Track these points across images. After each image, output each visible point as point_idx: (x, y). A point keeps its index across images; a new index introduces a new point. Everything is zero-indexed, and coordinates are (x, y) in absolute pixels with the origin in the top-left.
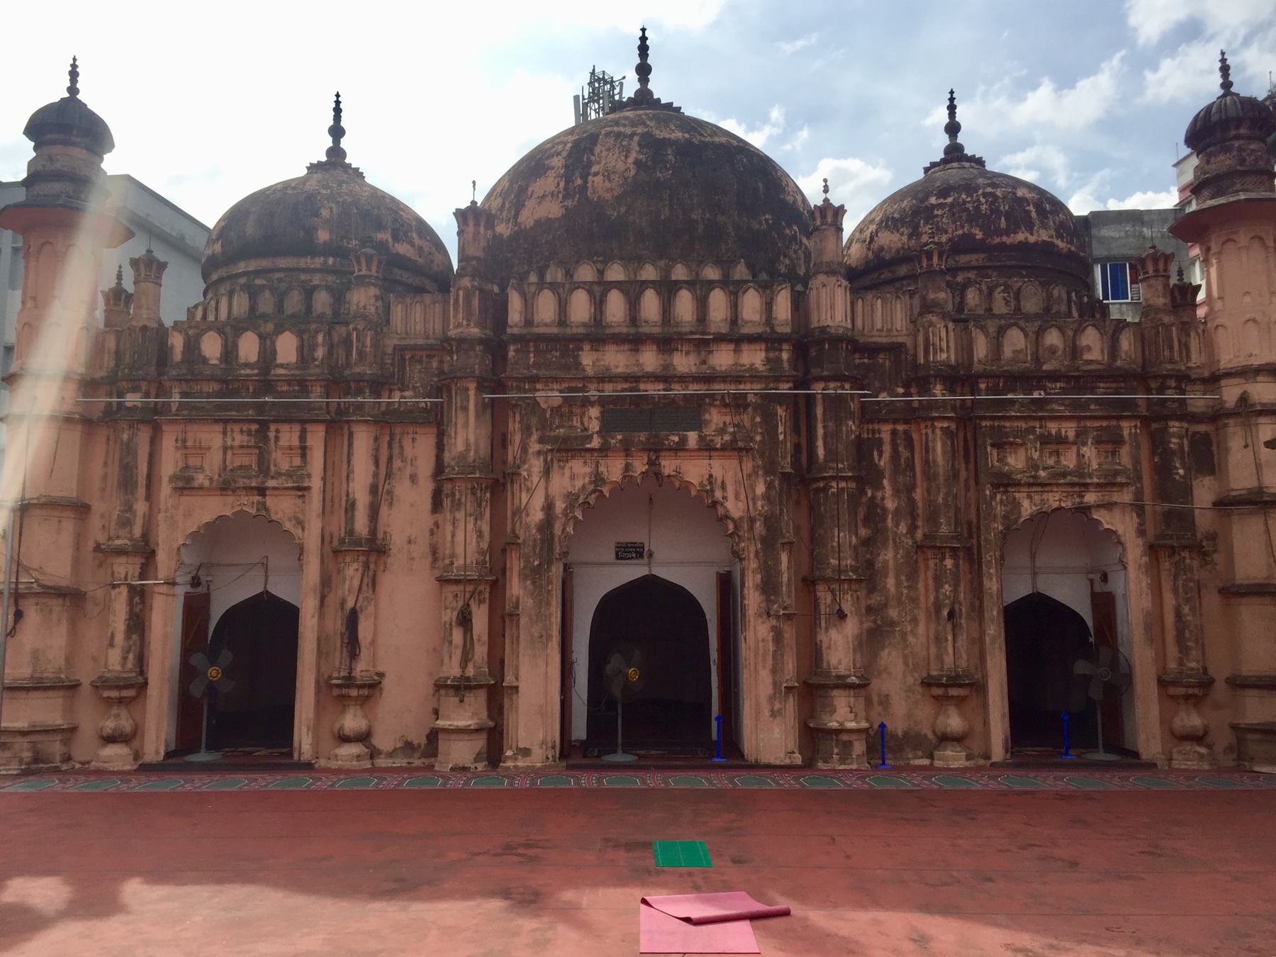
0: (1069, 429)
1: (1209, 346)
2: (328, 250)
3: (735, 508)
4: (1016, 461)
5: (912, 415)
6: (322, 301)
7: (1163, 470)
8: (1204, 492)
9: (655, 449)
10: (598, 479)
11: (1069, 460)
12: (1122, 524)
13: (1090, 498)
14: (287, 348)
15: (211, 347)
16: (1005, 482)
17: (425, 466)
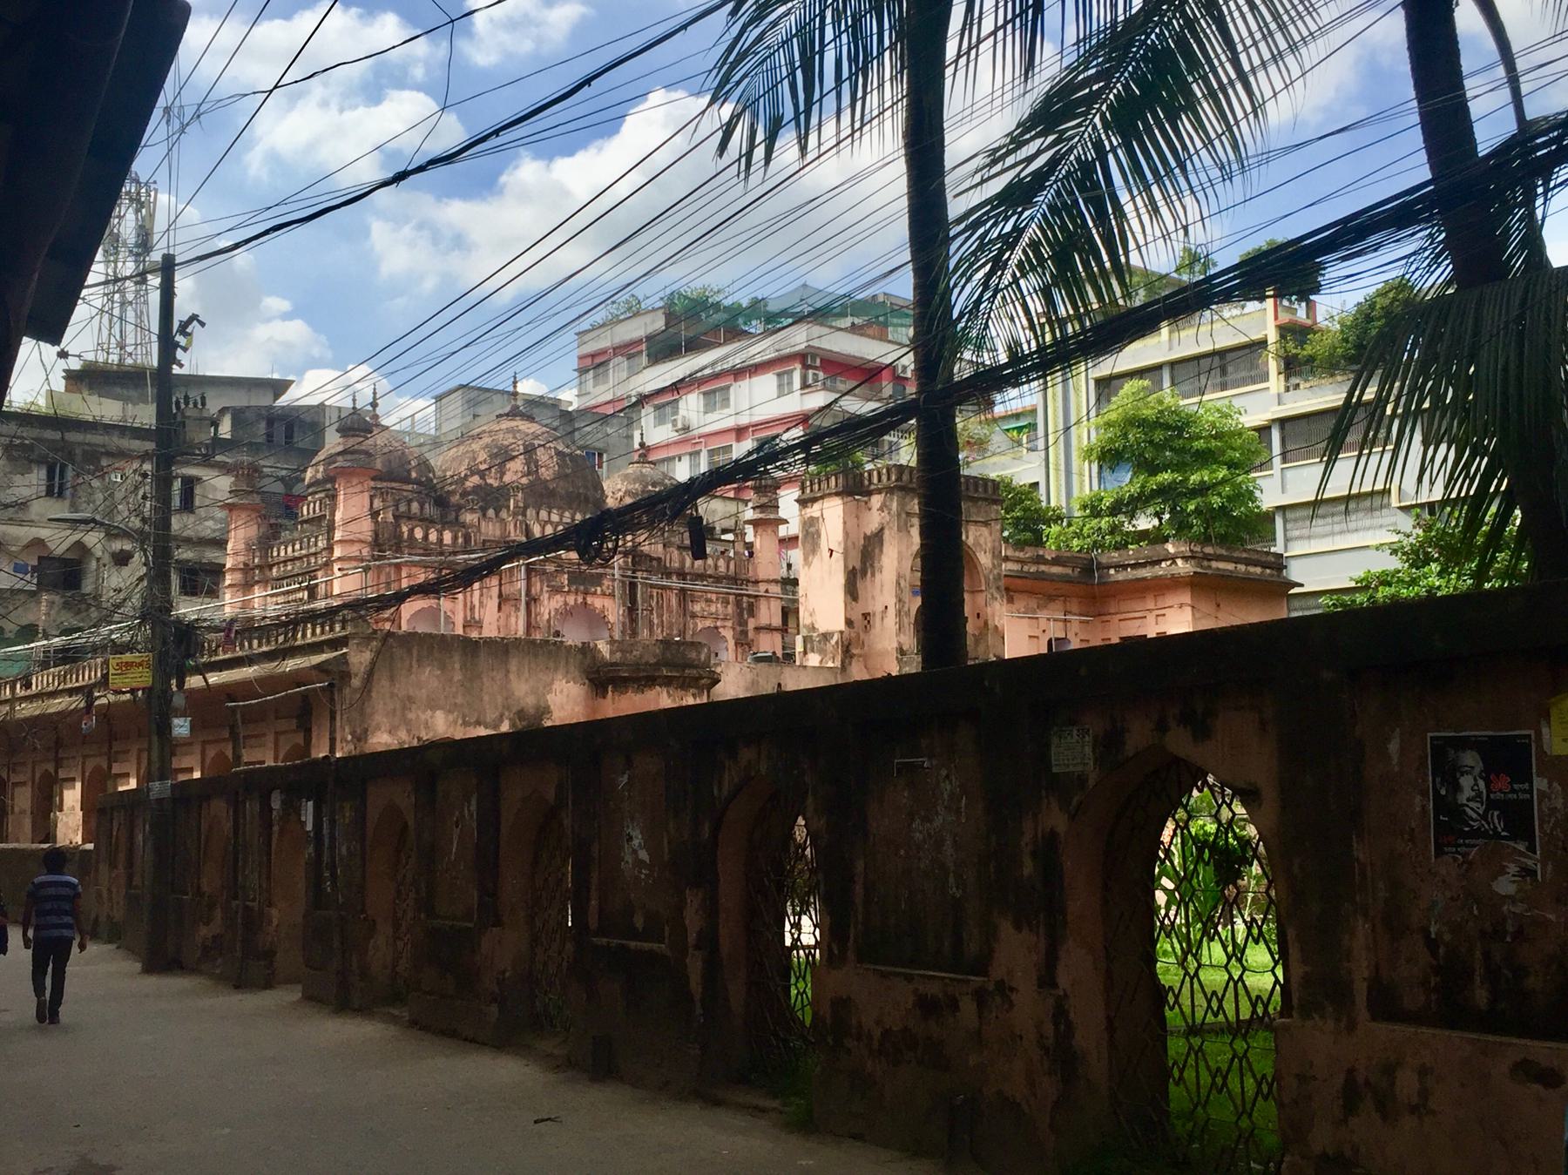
0: (714, 597)
1: (755, 570)
2: (418, 482)
3: (611, 618)
4: (697, 608)
5: (663, 588)
6: (415, 506)
7: (741, 614)
8: (752, 624)
9: (586, 593)
10: (566, 604)
11: (713, 609)
12: (728, 634)
13: (719, 623)
14: (447, 537)
15: (419, 534)
16: (694, 616)
17: (495, 591)
